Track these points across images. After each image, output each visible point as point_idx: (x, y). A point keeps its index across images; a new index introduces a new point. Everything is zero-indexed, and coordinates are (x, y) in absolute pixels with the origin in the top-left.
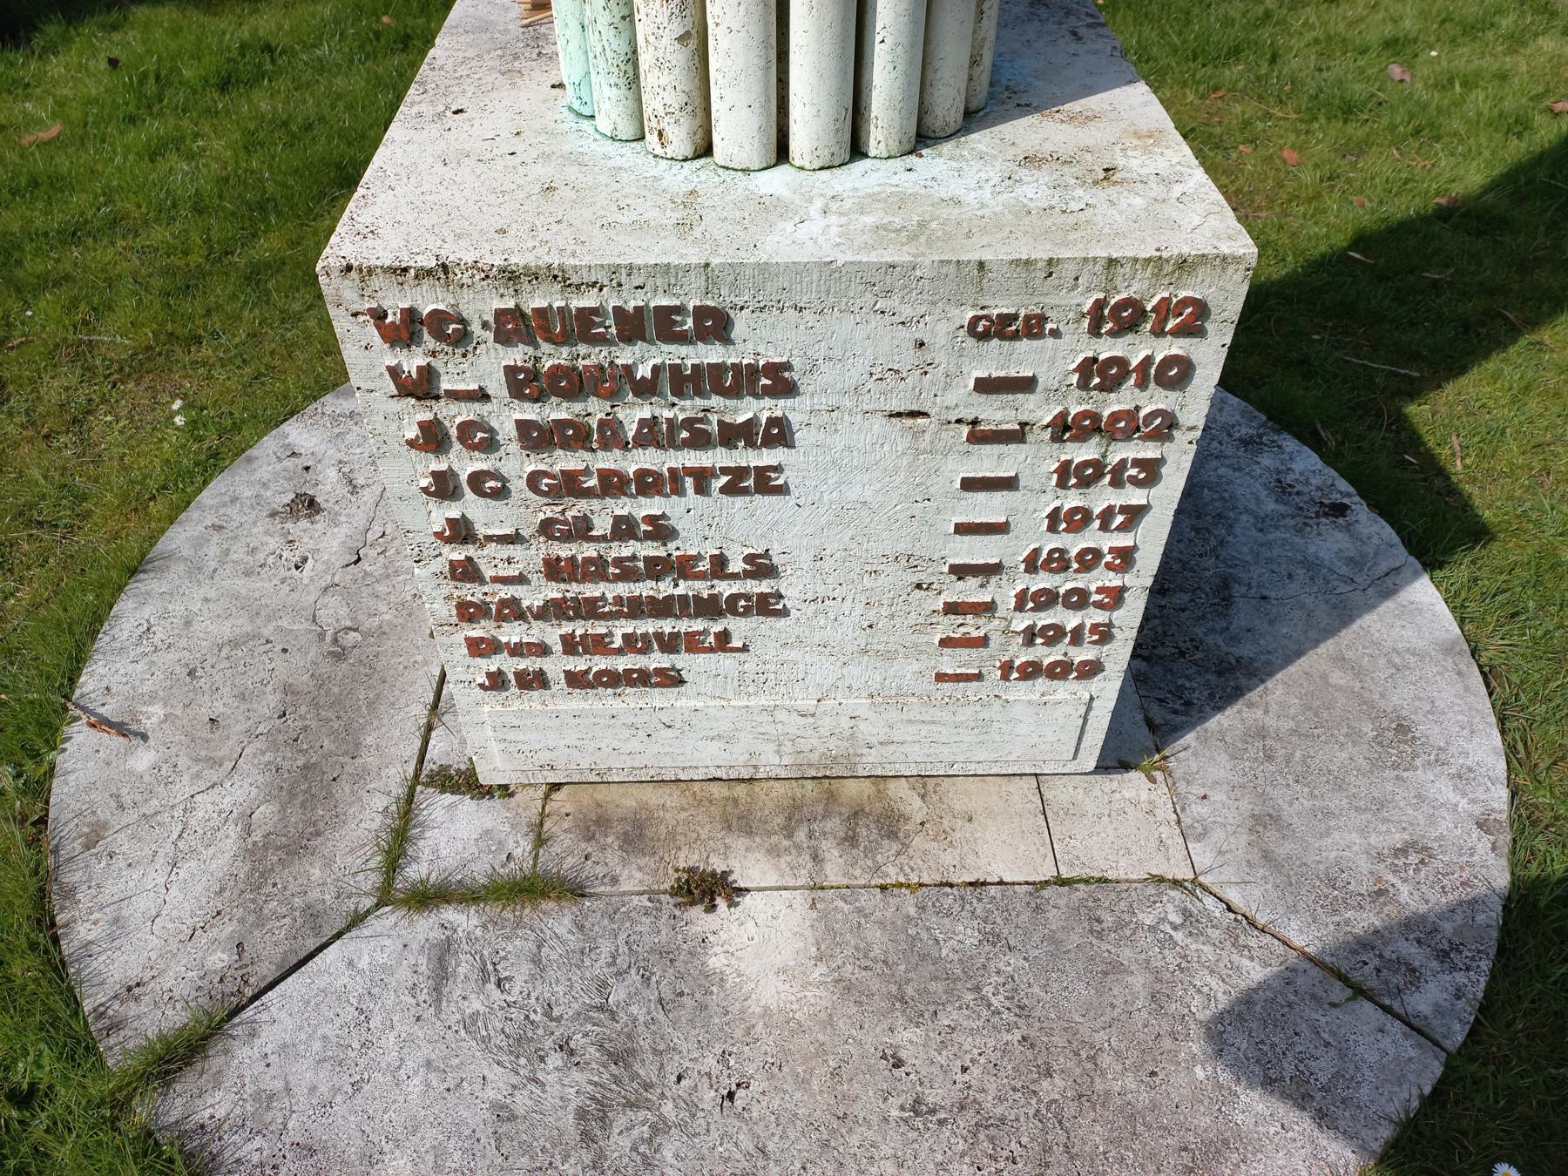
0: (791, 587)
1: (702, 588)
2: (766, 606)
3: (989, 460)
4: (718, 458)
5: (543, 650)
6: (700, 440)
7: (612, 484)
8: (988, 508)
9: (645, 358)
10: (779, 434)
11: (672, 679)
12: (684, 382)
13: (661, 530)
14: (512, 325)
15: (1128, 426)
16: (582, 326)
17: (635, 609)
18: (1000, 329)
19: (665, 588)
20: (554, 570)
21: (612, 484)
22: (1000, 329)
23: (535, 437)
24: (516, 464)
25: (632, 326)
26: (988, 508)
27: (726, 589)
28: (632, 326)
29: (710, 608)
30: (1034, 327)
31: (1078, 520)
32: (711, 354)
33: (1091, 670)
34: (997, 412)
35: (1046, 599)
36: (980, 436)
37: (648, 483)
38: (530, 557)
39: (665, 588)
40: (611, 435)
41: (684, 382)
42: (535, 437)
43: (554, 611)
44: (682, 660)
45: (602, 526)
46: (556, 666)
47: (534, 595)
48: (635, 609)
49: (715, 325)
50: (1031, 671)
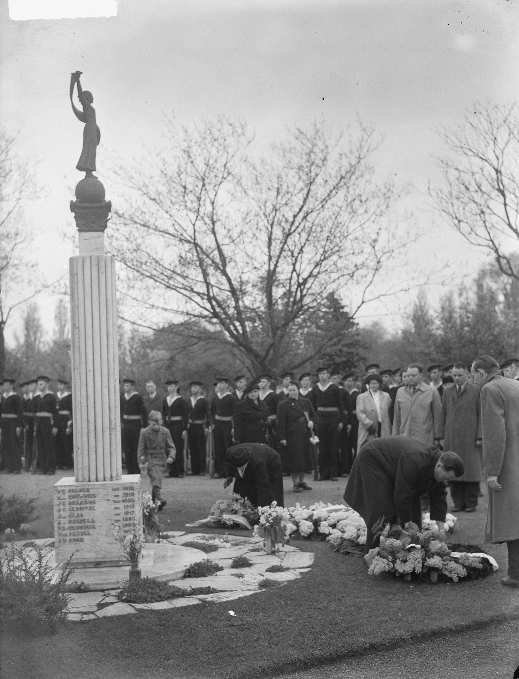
0: (96, 525)
1: (86, 524)
2: (94, 528)
3: (117, 505)
4: (88, 505)
5: (66, 535)
6: (87, 503)
7: (77, 509)
8: (118, 511)
9: (81, 494)
10: (94, 502)
11: (82, 540)
12: (86, 496)
13: (82, 516)
14: (70, 491)
16: (76, 491)
18: (114, 490)
20: (70, 522)
21: (77, 509)
22: (114, 490)
24: (67, 507)
25: (81, 490)
26: (118, 511)
27: (89, 524)
28: (81, 490)
30: (118, 489)
32: (87, 493)
34: (116, 499)
35: (126, 525)
36: (115, 502)
39: (82, 525)
41: (86, 496)
42: (70, 504)
44: (84, 537)
45: (76, 515)
46: (68, 538)
47: (67, 526)
49: (88, 490)
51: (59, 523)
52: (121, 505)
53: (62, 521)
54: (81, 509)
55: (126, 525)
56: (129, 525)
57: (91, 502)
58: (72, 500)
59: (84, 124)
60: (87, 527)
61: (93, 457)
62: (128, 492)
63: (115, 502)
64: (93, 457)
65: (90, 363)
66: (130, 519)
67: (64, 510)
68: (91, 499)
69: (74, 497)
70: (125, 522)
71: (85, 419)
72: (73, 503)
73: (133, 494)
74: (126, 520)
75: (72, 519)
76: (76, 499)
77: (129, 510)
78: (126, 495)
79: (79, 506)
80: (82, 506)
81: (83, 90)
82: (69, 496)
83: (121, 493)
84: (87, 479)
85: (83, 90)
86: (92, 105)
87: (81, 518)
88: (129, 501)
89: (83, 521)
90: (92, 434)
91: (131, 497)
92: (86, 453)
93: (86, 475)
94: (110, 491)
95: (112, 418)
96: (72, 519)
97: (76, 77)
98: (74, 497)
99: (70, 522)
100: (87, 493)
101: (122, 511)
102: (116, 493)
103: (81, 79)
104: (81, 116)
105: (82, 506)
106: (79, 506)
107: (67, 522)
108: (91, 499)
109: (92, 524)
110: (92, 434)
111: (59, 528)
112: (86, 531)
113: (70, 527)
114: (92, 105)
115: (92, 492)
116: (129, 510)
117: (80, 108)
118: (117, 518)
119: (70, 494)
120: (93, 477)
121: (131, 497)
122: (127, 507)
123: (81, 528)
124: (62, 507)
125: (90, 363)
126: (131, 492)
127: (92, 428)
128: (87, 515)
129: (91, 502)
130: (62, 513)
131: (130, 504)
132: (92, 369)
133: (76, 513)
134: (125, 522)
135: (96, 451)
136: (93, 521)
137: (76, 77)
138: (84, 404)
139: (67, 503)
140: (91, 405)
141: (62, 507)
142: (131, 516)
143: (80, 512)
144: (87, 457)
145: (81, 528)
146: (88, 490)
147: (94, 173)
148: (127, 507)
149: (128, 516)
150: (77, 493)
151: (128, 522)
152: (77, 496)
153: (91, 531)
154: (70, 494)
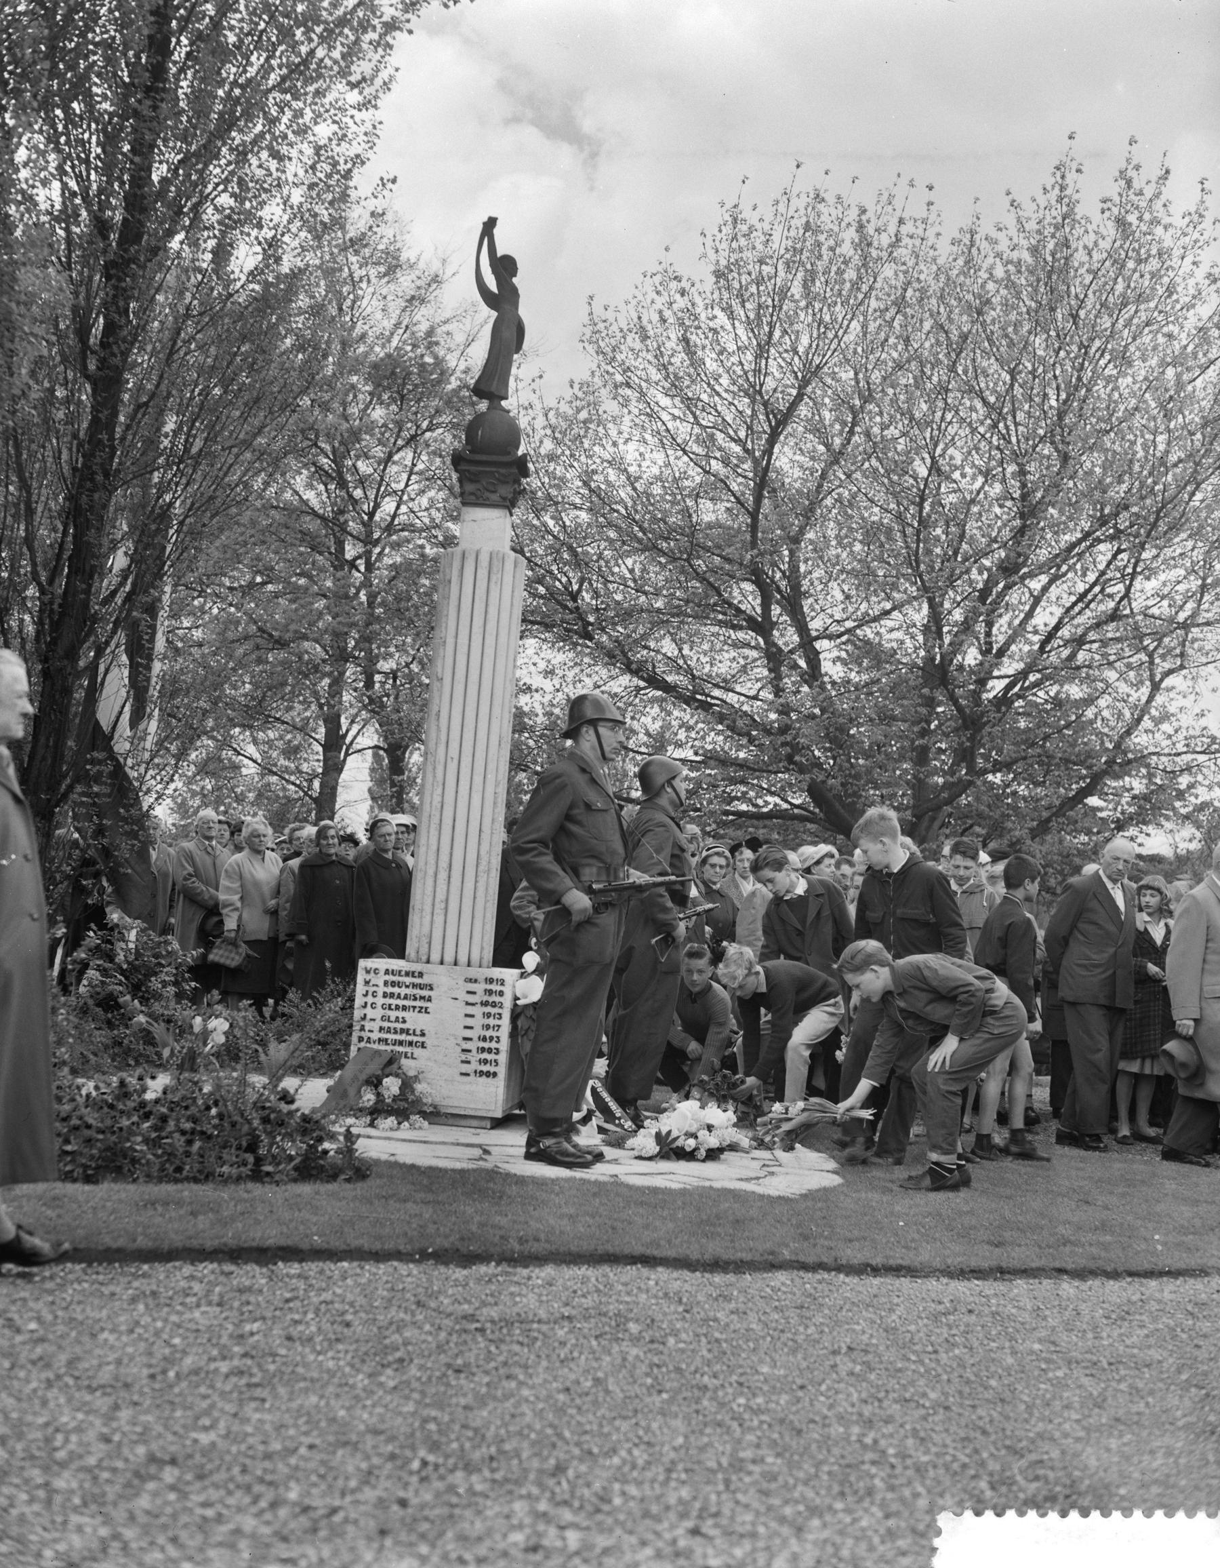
1: (409, 1038)
2: (423, 1046)
3: (470, 1010)
4: (418, 1003)
7: (397, 1007)
8: (469, 1022)
9: (408, 980)
10: (429, 1000)
12: (414, 986)
15: (494, 1005)
17: (395, 1043)
18: (471, 980)
19: (403, 1037)
21: (397, 1007)
22: (471, 980)
23: (385, 995)
24: (380, 1001)
25: (407, 974)
26: (469, 1022)
27: (415, 1039)
28: (407, 974)
29: (411, 1044)
31: (488, 1027)
33: (495, 1074)
34: (471, 999)
35: (483, 1050)
36: (467, 1004)
37: (404, 1008)
38: (375, 1026)
39: (403, 1037)
40: (399, 996)
41: (414, 986)
42: (385, 995)
47: (376, 1036)
48: (395, 1043)
49: (421, 975)
50: (481, 1073)
51: (362, 1029)
52: (478, 1011)
53: (368, 1026)
54: (404, 1008)
55: (483, 1050)
56: (490, 1051)
57: (422, 998)
58: (390, 990)
59: (494, 314)
60: (411, 1044)
61: (439, 919)
62: (494, 987)
63: (467, 1004)
64: (439, 919)
65: (454, 745)
66: (491, 1038)
67: (373, 1006)
68: (425, 993)
69: (393, 984)
70: (482, 1044)
71: (434, 848)
72: (392, 995)
73: (501, 994)
74: (484, 1039)
75: (386, 1024)
76: (396, 990)
77: (492, 1022)
78: (490, 992)
79: (401, 1003)
80: (406, 1003)
81: (499, 254)
82: (386, 983)
83: (480, 988)
84: (424, 958)
85: (499, 254)
86: (514, 280)
87: (399, 1026)
88: (494, 1005)
89: (407, 1032)
90: (443, 875)
91: (497, 999)
92: (428, 909)
93: (424, 950)
94: (461, 982)
95: (483, 853)
96: (386, 1024)
97: (490, 224)
98: (393, 984)
99: (381, 1029)
100: (417, 981)
101: (478, 1022)
102: (472, 987)
103: (496, 231)
104: (489, 298)
105: (406, 1003)
106: (401, 1003)
107: (376, 1028)
108: (425, 993)
109: (421, 1039)
110: (443, 875)
111: (361, 1039)
112: (409, 1049)
113: (380, 1040)
114: (514, 280)
115: (425, 980)
116: (492, 1022)
117: (491, 283)
118: (468, 1033)
119: (387, 977)
120: (435, 957)
121: (497, 999)
122: (489, 1015)
123: (401, 1043)
124: (370, 999)
125: (454, 745)
126: (499, 988)
127: (444, 864)
128: (414, 1020)
129: (422, 998)
130: (369, 1011)
131: (493, 1011)
132: (456, 757)
133: (393, 1014)
134: (482, 1044)
135: (446, 909)
136: (423, 1035)
137: (490, 224)
138: (436, 820)
139: (380, 994)
140: (447, 821)
141: (370, 999)
142: (494, 1034)
143: (401, 1014)
144: (428, 918)
145: (401, 1043)
146: (421, 975)
147: (503, 403)
148: (489, 1015)
149: (488, 1034)
150: (401, 979)
151: (486, 1045)
152: (399, 985)
153: (418, 1052)
154: (387, 977)
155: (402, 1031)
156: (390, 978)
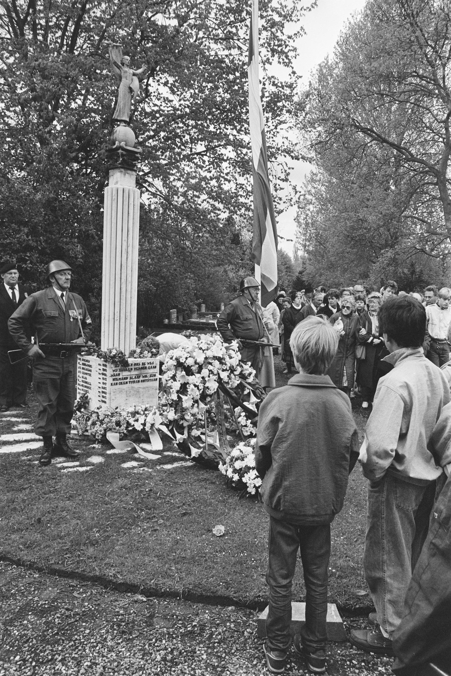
0: (92, 387)
4: (89, 372)
9: (87, 363)
10: (90, 371)
35: (103, 392)
43: (82, 385)
54: (86, 374)
60: (88, 387)
89: (86, 382)
91: (105, 372)
100: (89, 364)
123: (86, 387)
128: (89, 379)
133: (85, 376)
145: (86, 387)
151: (104, 390)
155: (86, 382)
156: (83, 362)
